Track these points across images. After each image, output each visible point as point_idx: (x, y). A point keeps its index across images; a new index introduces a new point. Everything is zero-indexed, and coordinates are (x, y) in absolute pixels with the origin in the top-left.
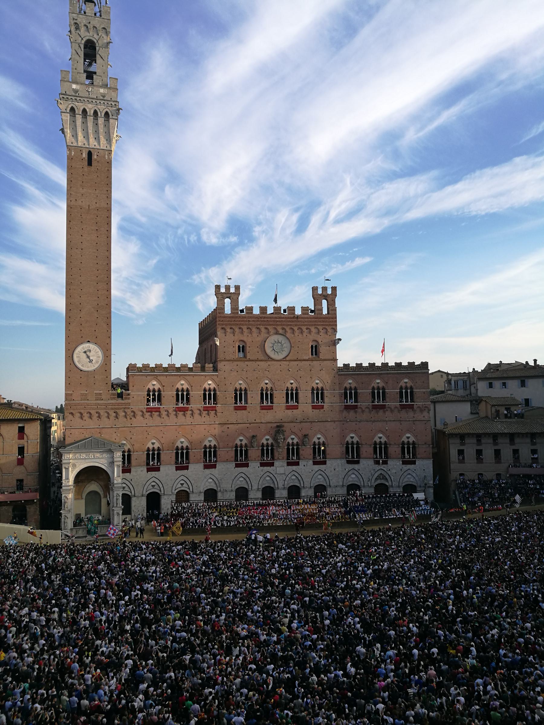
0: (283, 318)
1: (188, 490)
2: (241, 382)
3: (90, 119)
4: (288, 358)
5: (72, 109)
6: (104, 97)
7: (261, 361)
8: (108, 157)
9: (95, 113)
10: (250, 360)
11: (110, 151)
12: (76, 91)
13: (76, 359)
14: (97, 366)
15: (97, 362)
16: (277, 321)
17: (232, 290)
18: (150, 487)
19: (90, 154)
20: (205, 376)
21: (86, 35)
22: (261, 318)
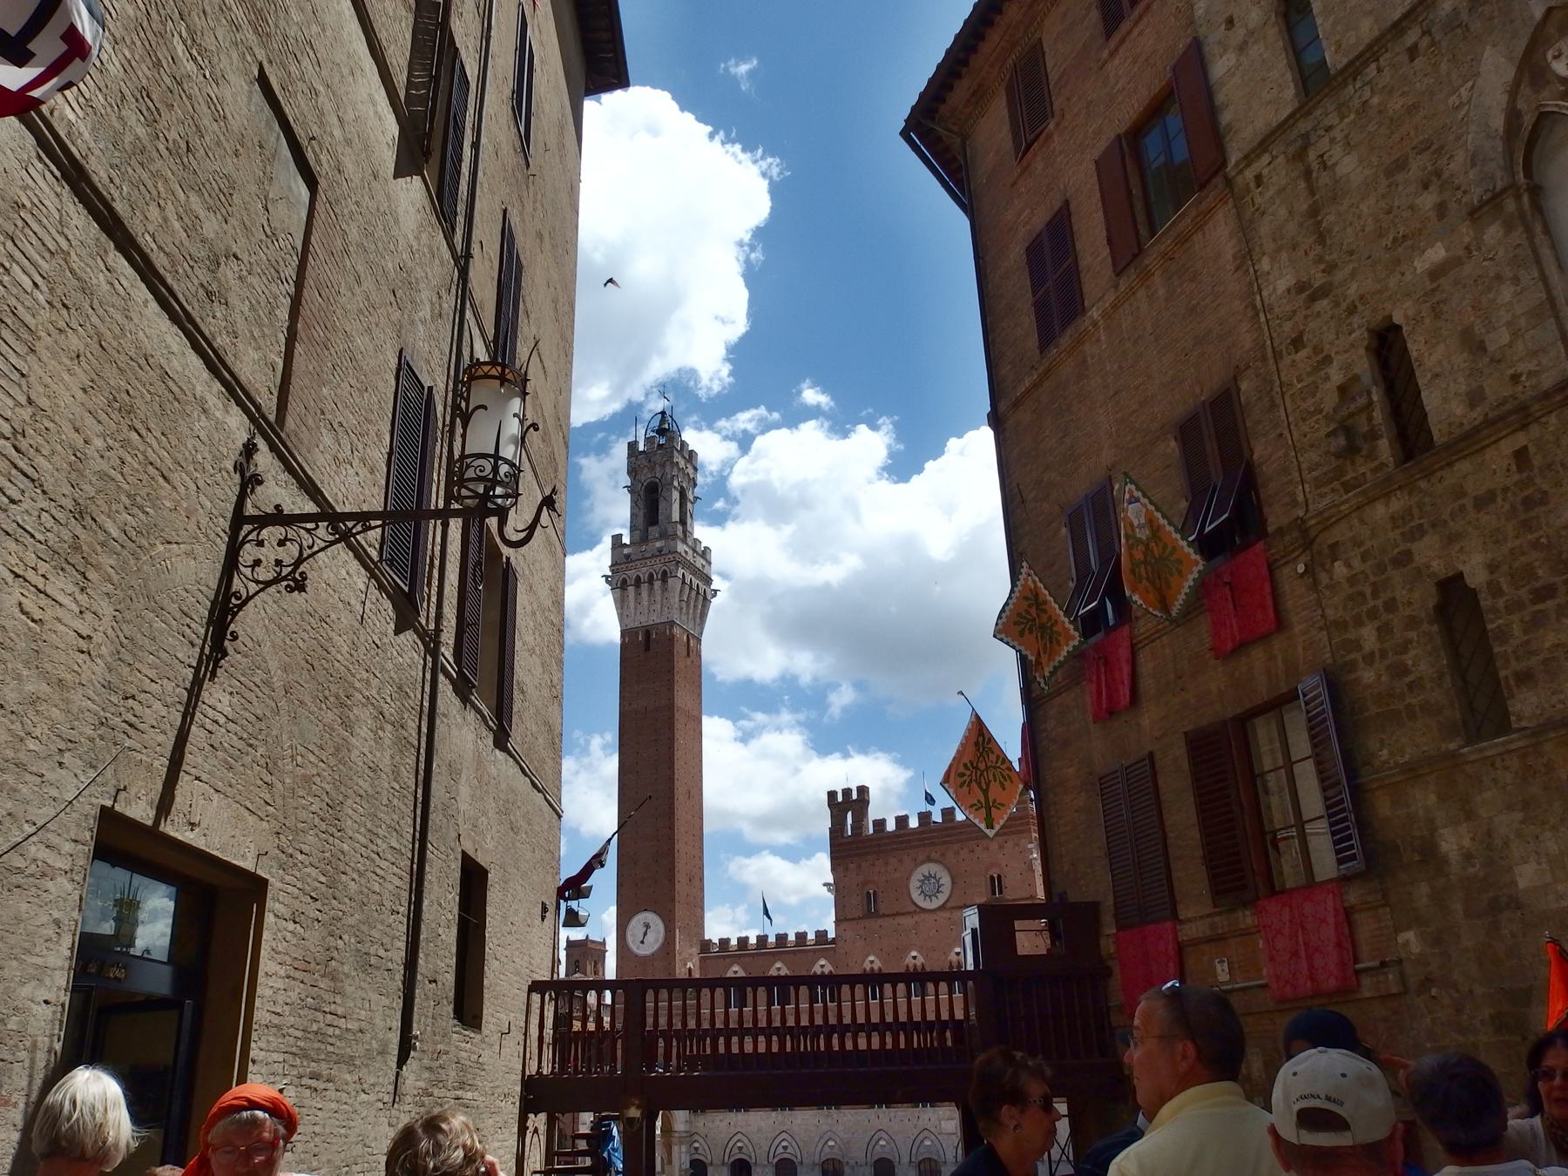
0: (934, 831)
1: (794, 1159)
2: (871, 958)
3: (645, 588)
4: (949, 905)
5: (624, 581)
6: (660, 551)
7: (903, 914)
8: (670, 631)
9: (651, 576)
10: (884, 916)
11: (672, 623)
12: (628, 556)
13: (630, 939)
14: (656, 947)
15: (657, 941)
16: (925, 839)
17: (855, 796)
18: (736, 1150)
19: (647, 634)
20: (814, 951)
21: (646, 477)
22: (898, 836)
